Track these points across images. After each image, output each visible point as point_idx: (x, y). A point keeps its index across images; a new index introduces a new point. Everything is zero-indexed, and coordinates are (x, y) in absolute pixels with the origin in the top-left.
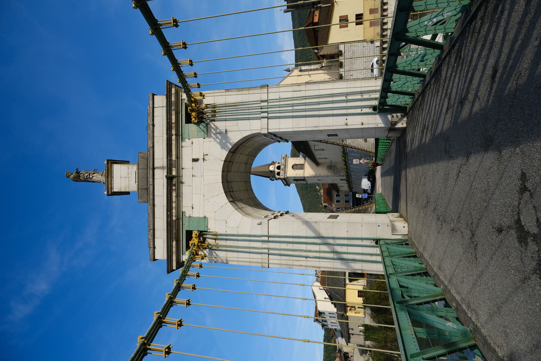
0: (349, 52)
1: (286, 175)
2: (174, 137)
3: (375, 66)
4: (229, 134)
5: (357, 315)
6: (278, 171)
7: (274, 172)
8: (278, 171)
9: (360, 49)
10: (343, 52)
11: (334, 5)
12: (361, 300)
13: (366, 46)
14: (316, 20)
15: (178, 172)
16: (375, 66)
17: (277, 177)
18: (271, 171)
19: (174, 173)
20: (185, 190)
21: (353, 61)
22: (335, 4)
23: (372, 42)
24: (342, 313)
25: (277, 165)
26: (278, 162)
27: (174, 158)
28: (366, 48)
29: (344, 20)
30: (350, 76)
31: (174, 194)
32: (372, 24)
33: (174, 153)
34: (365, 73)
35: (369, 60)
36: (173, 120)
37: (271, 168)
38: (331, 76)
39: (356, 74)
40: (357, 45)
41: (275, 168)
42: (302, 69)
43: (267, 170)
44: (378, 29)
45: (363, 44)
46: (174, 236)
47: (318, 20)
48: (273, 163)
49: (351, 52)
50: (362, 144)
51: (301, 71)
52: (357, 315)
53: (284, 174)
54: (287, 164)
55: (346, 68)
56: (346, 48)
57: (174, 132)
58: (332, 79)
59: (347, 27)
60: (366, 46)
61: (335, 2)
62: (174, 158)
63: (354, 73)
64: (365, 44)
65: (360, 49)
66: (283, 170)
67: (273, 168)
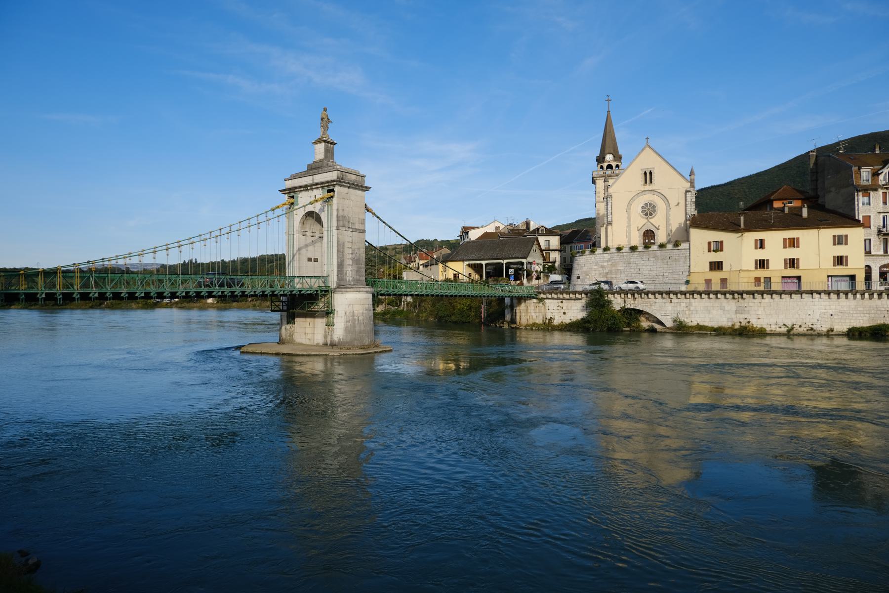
0: (678, 255)
1: (598, 178)
2: (320, 186)
3: (633, 286)
4: (323, 213)
5: (440, 273)
6: (605, 167)
7: (603, 162)
8: (605, 167)
9: (680, 268)
10: (679, 248)
11: (739, 233)
12: (451, 277)
13: (683, 275)
14: (777, 204)
15: (309, 189)
16: (633, 286)
17: (599, 166)
18: (604, 158)
19: (309, 188)
20: (306, 193)
21: (666, 261)
22: (740, 234)
23: (687, 282)
24: (441, 259)
25: (614, 164)
26: (619, 164)
27: (313, 187)
28: (681, 276)
29: (719, 247)
30: (648, 257)
31: (302, 189)
32: (708, 282)
33: (315, 187)
34: (651, 275)
35: (666, 279)
36: (326, 185)
37: (609, 157)
38: (674, 232)
39: (650, 264)
40: (685, 265)
41: (609, 162)
42: (688, 193)
43: (607, 151)
44: (702, 288)
45: (685, 272)
46: (292, 191)
47: (774, 208)
48: (618, 158)
49: (677, 258)
50: (576, 273)
51: (686, 192)
52: (440, 273)
53: (599, 176)
54: (612, 177)
55: (658, 252)
56: (683, 251)
57: (322, 185)
58: (671, 234)
59: (708, 252)
60: (683, 275)
61: (742, 234)
62: (313, 187)
63: (652, 262)
64: (687, 273)
65: (680, 268)
66: (604, 173)
67: (609, 160)
